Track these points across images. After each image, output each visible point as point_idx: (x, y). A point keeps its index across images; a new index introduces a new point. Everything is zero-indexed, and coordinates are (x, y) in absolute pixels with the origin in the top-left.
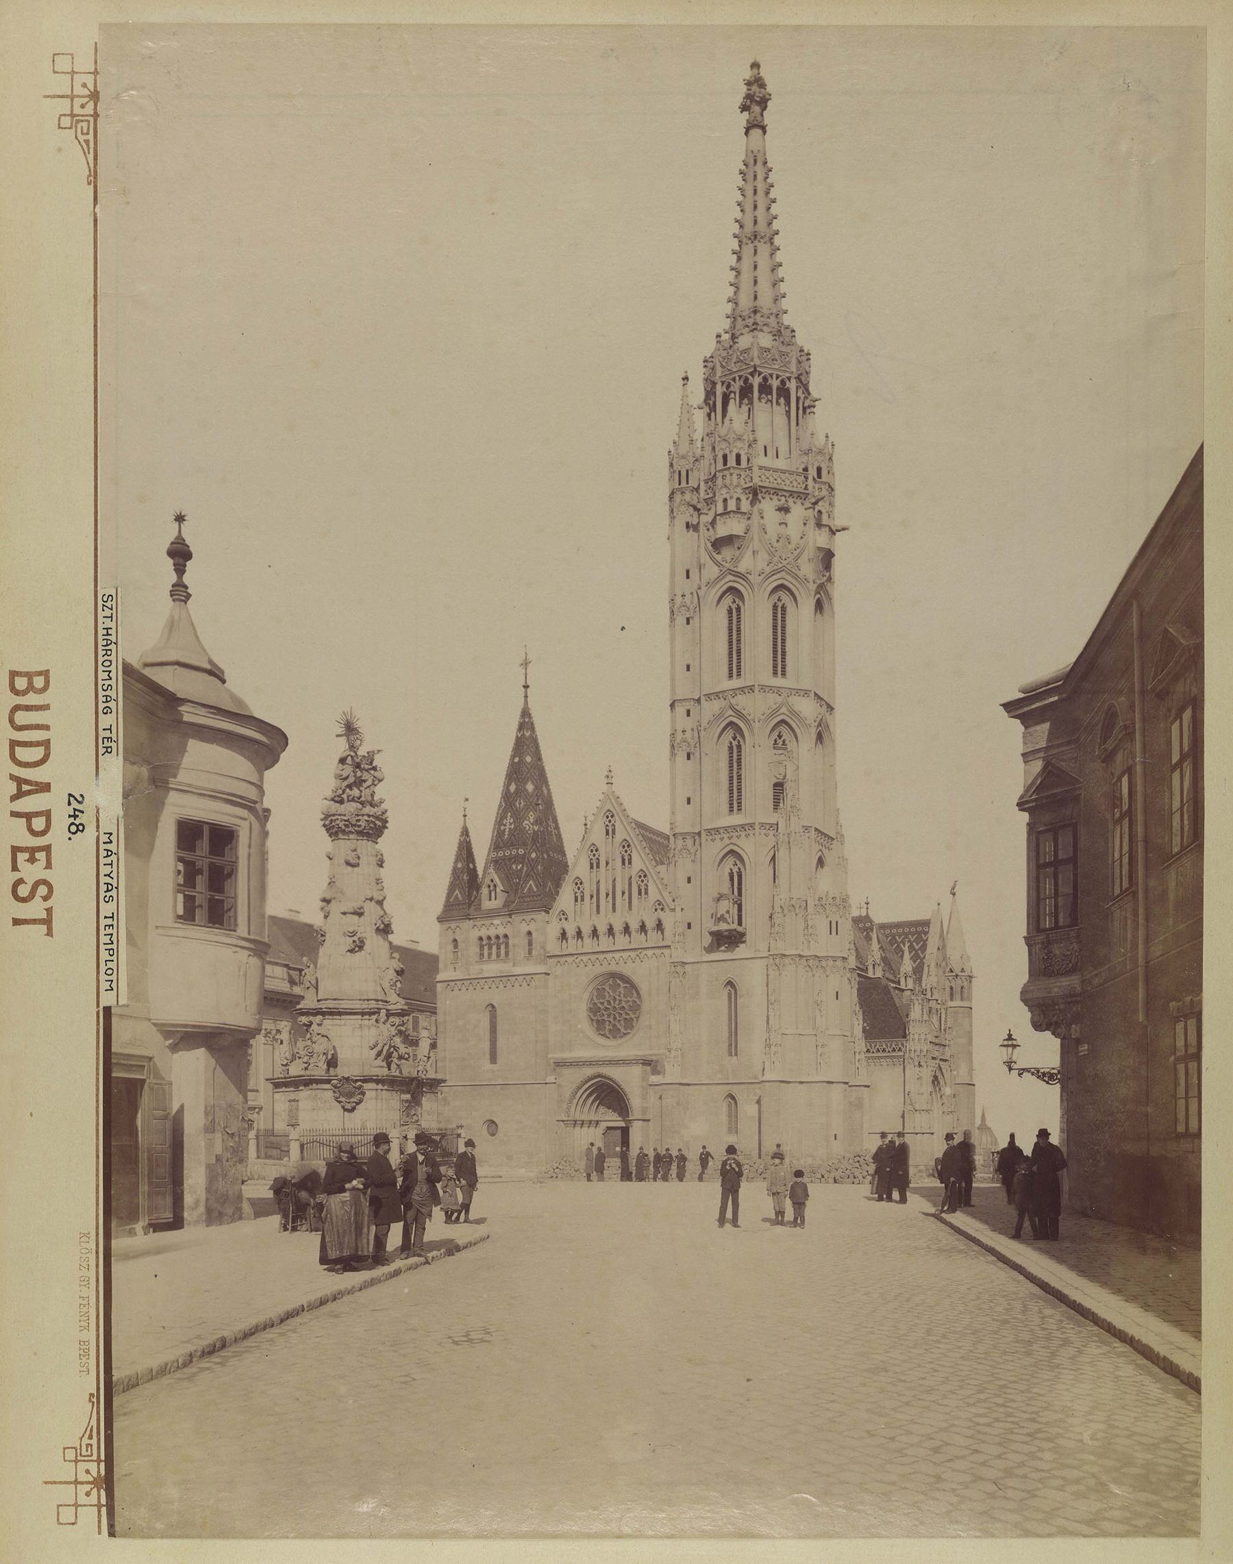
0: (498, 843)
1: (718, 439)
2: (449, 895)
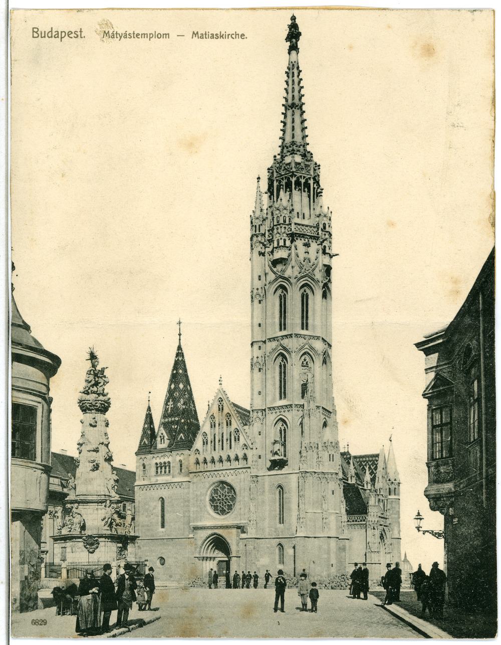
1: (274, 209)
2: (142, 440)
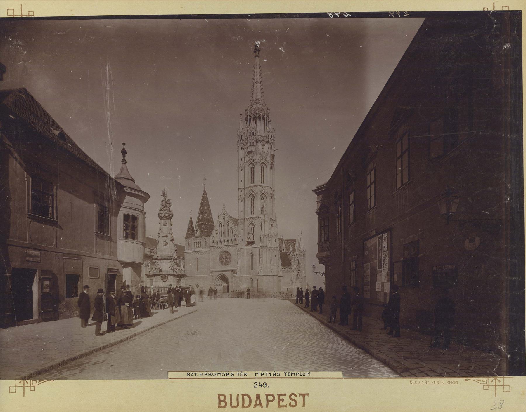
0: (199, 221)
2: (187, 232)
